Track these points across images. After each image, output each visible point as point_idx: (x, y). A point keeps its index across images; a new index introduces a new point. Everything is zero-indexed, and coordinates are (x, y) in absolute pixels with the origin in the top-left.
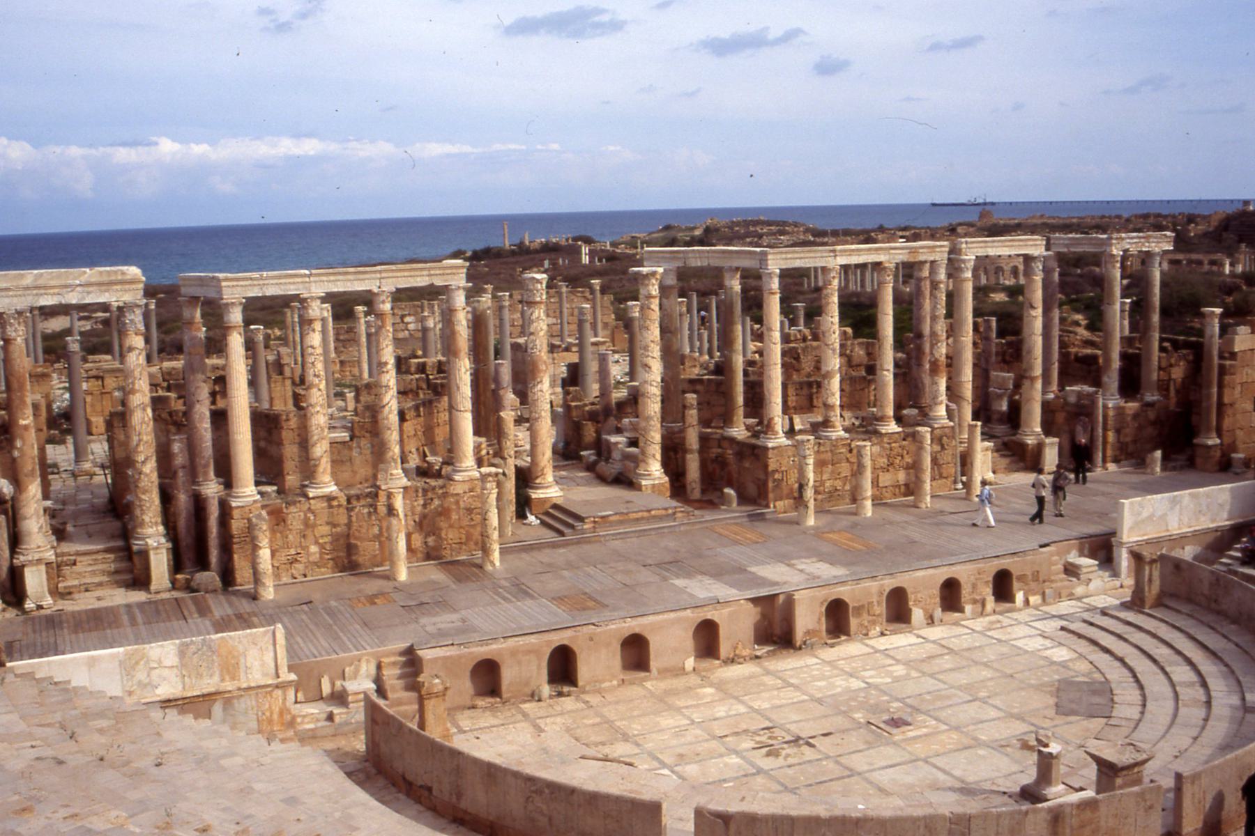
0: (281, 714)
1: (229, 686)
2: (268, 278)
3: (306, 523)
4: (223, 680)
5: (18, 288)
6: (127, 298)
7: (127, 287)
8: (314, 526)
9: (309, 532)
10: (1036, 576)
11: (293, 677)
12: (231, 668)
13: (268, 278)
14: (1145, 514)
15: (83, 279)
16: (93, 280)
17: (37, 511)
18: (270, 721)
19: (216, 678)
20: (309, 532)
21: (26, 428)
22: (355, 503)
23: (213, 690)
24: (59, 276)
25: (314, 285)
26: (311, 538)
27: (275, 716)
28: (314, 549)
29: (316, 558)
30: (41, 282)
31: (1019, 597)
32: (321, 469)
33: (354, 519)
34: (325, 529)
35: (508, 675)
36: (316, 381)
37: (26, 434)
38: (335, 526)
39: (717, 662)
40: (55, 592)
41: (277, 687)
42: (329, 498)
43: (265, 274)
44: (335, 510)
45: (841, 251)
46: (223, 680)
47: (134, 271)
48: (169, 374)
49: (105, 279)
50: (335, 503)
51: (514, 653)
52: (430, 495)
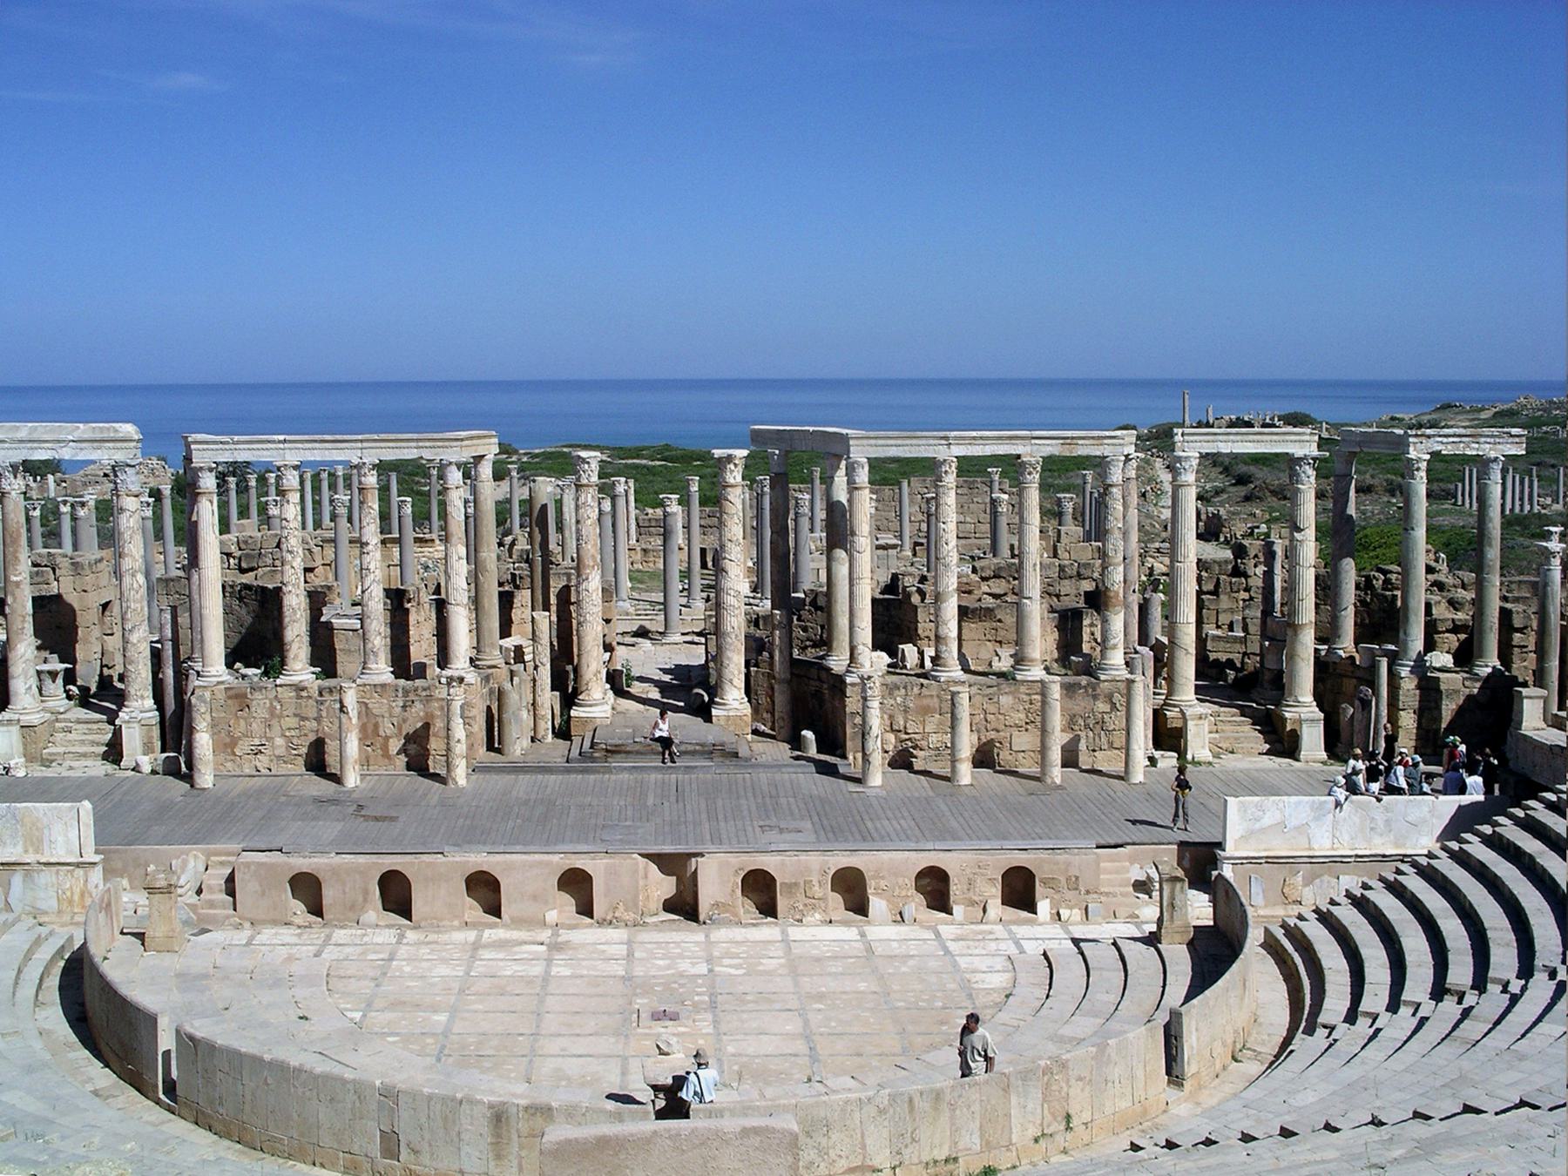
0: (82, 895)
1: (30, 858)
2: (238, 442)
3: (272, 709)
4: (26, 851)
5: (13, 441)
6: (119, 456)
7: (119, 445)
8: (281, 717)
9: (274, 722)
10: (1074, 884)
11: (97, 858)
12: (35, 840)
13: (238, 442)
14: (1267, 820)
15: (76, 435)
16: (86, 436)
17: (25, 672)
18: (71, 902)
19: (20, 849)
20: (274, 722)
21: (18, 584)
22: (327, 696)
23: (12, 860)
24: (52, 431)
25: (286, 453)
26: (276, 728)
27: (76, 898)
28: (279, 741)
29: (281, 751)
30: (35, 436)
31: (1043, 906)
32: (291, 655)
33: (324, 714)
34: (292, 722)
35: (329, 895)
36: (289, 557)
37: (17, 592)
38: (303, 719)
39: (588, 920)
40: (30, 758)
41: (78, 865)
42: (299, 688)
43: (236, 438)
44: (303, 702)
45: (956, 438)
46: (26, 851)
47: (129, 429)
48: (246, 542)
49: (98, 436)
50: (304, 694)
51: (335, 871)
52: (412, 697)
